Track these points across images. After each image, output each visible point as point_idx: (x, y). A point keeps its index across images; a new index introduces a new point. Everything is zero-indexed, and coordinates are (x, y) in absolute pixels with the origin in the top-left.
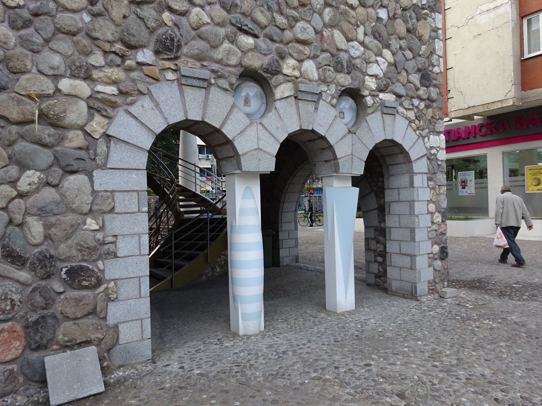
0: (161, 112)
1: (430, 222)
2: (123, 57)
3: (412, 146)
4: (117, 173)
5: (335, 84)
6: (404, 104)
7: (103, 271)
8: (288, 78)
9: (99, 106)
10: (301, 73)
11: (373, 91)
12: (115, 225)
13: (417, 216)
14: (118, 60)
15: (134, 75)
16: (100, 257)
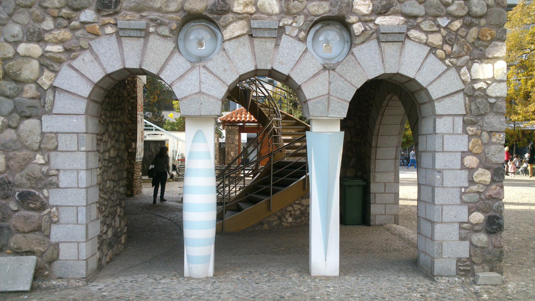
0: (100, 64)
1: (466, 180)
2: (69, 19)
3: (435, 80)
4: (60, 118)
5: (304, 14)
6: (422, 26)
7: (47, 198)
8: (239, 16)
9: (48, 63)
10: (257, 8)
11: (366, 15)
12: (58, 160)
13: (439, 171)
14: (65, 22)
15: (79, 33)
16: (45, 186)
